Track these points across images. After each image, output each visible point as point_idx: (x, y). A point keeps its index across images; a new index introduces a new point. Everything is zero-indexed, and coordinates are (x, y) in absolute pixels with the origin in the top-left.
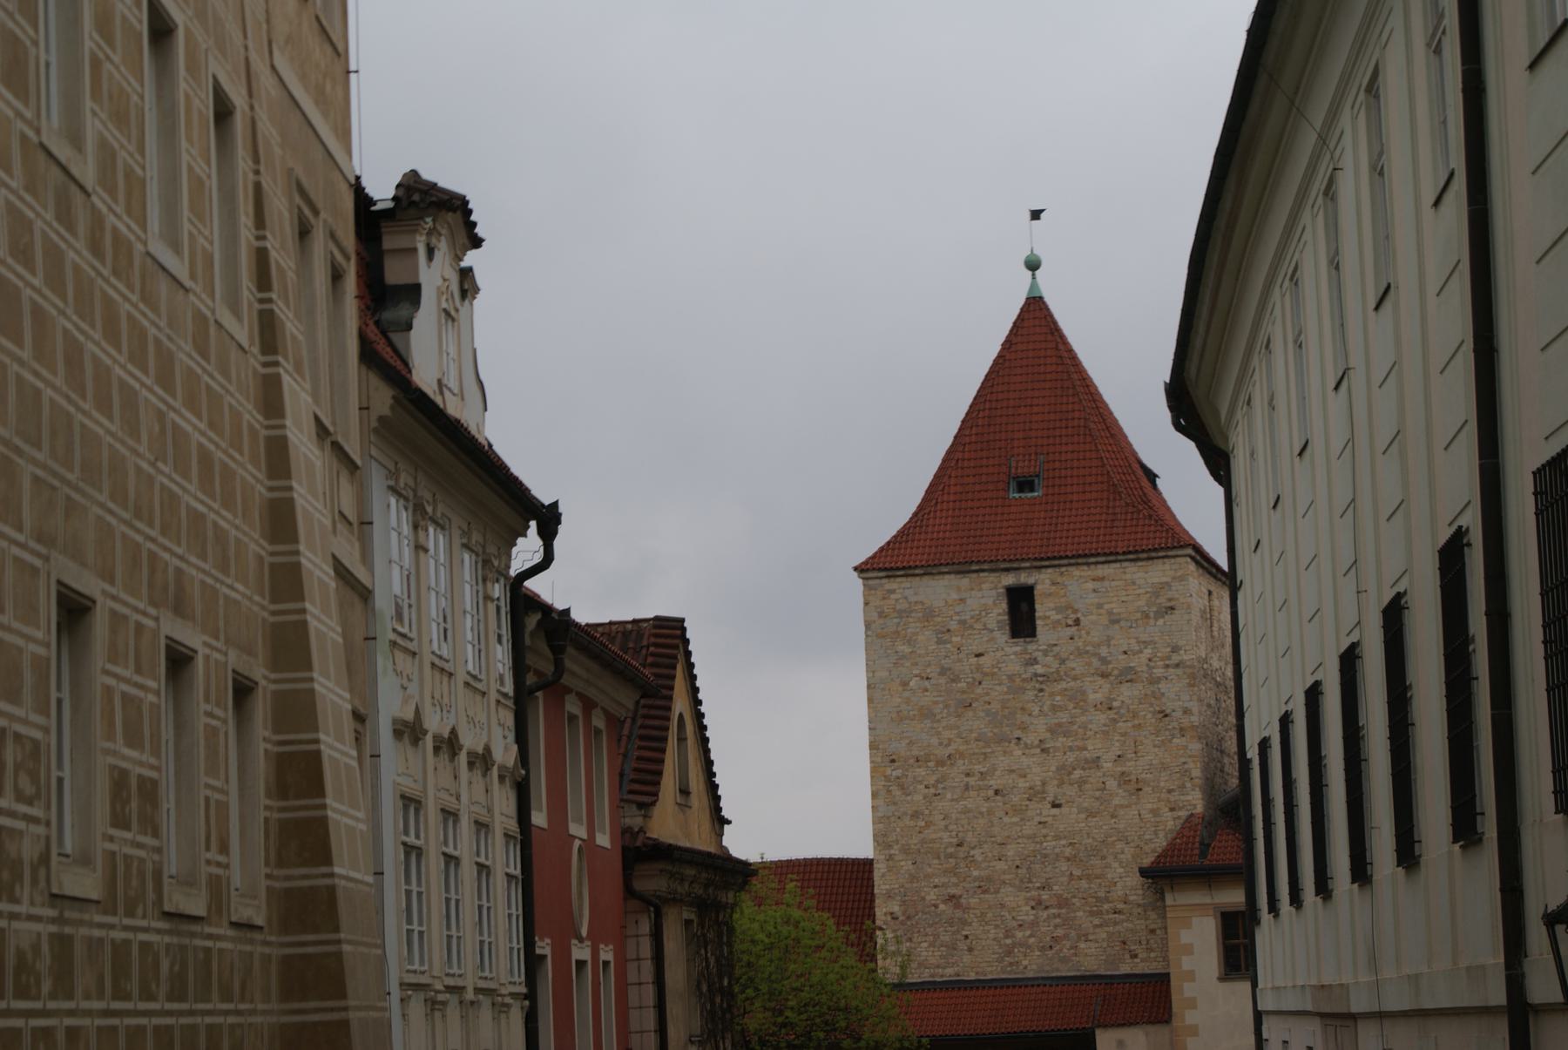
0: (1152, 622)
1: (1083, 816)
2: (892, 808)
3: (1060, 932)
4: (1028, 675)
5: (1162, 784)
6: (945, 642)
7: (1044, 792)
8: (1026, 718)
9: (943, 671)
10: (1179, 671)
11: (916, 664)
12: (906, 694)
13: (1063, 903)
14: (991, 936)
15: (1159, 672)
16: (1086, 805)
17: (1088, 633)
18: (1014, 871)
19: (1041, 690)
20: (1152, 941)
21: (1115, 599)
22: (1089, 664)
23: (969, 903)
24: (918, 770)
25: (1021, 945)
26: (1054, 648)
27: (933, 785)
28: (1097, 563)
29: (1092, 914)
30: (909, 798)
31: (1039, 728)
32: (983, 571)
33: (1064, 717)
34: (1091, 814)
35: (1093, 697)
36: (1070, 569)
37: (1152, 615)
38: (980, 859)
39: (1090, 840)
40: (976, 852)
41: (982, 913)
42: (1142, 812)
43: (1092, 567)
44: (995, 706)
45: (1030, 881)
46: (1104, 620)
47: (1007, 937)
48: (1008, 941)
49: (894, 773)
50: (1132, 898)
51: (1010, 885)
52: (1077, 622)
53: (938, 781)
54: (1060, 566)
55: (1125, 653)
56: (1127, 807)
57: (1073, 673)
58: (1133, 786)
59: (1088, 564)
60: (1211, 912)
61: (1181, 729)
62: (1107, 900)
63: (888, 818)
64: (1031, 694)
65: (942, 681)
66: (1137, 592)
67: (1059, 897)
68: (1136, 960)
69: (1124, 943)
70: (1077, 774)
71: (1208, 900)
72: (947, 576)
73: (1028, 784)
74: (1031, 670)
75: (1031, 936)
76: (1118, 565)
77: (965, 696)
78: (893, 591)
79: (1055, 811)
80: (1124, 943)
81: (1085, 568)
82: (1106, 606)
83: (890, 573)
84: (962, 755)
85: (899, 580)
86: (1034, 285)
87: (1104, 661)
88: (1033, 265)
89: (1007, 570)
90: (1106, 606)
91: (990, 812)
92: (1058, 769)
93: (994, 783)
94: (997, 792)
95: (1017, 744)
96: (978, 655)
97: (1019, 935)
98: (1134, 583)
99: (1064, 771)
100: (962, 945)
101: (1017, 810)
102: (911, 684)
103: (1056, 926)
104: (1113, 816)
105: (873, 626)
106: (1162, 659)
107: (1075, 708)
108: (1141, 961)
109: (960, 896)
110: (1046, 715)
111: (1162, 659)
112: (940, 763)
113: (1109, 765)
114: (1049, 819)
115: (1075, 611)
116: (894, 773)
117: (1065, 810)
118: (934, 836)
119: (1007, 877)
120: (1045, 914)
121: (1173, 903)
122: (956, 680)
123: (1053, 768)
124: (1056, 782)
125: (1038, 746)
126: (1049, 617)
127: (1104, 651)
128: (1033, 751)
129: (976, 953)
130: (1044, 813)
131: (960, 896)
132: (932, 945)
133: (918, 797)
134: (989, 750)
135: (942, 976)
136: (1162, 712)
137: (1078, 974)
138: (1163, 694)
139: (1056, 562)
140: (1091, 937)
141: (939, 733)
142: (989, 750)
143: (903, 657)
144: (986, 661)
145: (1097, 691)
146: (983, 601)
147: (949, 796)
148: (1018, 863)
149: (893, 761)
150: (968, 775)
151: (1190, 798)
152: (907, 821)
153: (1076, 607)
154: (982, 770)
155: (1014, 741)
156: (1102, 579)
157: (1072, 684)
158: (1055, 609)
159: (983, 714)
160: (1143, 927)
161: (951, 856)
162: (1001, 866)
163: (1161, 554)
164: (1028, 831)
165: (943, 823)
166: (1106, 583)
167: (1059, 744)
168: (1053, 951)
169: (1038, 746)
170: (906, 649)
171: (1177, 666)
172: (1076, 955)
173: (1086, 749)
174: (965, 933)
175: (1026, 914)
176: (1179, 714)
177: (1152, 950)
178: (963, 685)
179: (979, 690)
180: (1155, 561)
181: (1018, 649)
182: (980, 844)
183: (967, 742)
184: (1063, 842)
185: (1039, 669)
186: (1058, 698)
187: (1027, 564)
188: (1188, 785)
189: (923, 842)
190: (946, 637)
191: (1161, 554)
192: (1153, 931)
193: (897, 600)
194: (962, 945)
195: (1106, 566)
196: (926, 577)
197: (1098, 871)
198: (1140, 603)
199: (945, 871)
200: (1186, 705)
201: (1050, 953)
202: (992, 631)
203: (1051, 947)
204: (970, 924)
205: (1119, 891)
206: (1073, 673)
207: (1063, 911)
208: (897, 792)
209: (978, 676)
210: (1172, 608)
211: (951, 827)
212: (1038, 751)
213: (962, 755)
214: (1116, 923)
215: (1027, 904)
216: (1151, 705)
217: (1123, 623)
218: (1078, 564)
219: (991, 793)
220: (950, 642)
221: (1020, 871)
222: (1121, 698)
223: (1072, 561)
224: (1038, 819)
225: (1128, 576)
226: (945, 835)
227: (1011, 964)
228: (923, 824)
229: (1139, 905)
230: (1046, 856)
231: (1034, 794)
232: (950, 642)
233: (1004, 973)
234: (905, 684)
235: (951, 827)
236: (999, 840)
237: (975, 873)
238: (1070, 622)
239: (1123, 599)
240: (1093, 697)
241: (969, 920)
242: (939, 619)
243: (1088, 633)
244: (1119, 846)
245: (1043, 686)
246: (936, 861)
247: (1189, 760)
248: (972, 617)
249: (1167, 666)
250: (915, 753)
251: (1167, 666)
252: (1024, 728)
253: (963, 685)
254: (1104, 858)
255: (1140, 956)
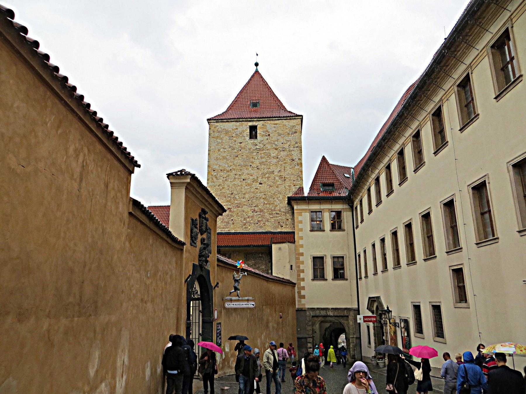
0: (290, 135)
1: (268, 187)
2: (213, 183)
3: (260, 219)
4: (255, 149)
5: (292, 179)
6: (231, 139)
7: (257, 180)
8: (253, 160)
9: (230, 147)
10: (298, 149)
11: (223, 145)
12: (219, 153)
13: (261, 211)
14: (239, 220)
15: (292, 149)
16: (269, 184)
17: (272, 138)
18: (247, 202)
19: (258, 153)
20: (287, 222)
21: (280, 129)
22: (272, 146)
23: (234, 210)
24: (221, 173)
25: (248, 222)
26: (262, 142)
27: (225, 178)
28: (276, 120)
29: (270, 214)
30: (218, 181)
31: (257, 162)
32: (243, 121)
33: (264, 160)
34: (271, 186)
35: (272, 155)
36: (268, 121)
37: (290, 134)
38: (237, 198)
39: (270, 194)
40: (237, 197)
41: (237, 213)
42: (286, 186)
43: (274, 121)
44: (245, 156)
45: (252, 204)
46: (277, 135)
47: (244, 220)
48: (245, 221)
49: (214, 174)
50: (282, 210)
51: (246, 205)
52: (269, 135)
53: (227, 176)
54: (265, 120)
55: (282, 143)
56: (281, 184)
57: (267, 148)
58: (283, 179)
59: (273, 120)
60: (308, 211)
61: (298, 164)
62: (274, 210)
63: (212, 186)
64: (255, 154)
65: (230, 149)
66: (287, 128)
67: (260, 209)
68: (282, 228)
69: (279, 223)
70: (267, 175)
71: (307, 208)
72: (233, 122)
73: (253, 178)
74: (255, 147)
75: (251, 220)
76: (281, 121)
77: (236, 154)
78: (217, 126)
79: (261, 185)
80: (279, 223)
81: (272, 121)
82: (277, 131)
83: (217, 121)
84: (234, 170)
85: (219, 123)
86: (257, 69)
87: (276, 145)
88: (257, 65)
89: (250, 121)
90: (277, 131)
91: (241, 185)
92: (262, 174)
93: (243, 177)
94: (243, 180)
95: (250, 167)
96: (240, 143)
97: (248, 220)
98: (285, 125)
99: (263, 175)
100: (231, 222)
101: (249, 185)
102: (221, 150)
103: (259, 217)
104: (277, 187)
105: (211, 135)
106: (293, 145)
107: (267, 158)
108: (284, 228)
109: (231, 208)
110: (259, 159)
111: (293, 145)
112: (228, 171)
113: (277, 173)
114: (259, 188)
115: (269, 132)
116: (214, 174)
117: (263, 185)
118: (225, 191)
119: (245, 203)
120: (256, 214)
121: (297, 208)
122: (234, 149)
123: (260, 174)
124: (261, 177)
125: (256, 168)
126: (261, 134)
127: (276, 143)
128: (255, 169)
129: (235, 224)
130: (257, 186)
131: (231, 208)
132: (222, 222)
133: (221, 181)
134: (242, 168)
135: (224, 231)
136: (292, 159)
137: (265, 231)
138: (293, 154)
139: (264, 119)
140: (269, 221)
141: (228, 163)
142: (242, 168)
143: (219, 143)
144: (243, 145)
145: (274, 153)
146: (243, 129)
147: (230, 180)
148: (249, 199)
149: (214, 171)
150: (236, 175)
151: (300, 183)
152: (217, 187)
153: (269, 131)
154: (240, 174)
155: (249, 166)
156: (277, 124)
157: (267, 151)
158: (263, 132)
159: (241, 159)
160: (285, 218)
161: (229, 197)
162: (244, 200)
163: (293, 118)
164: (252, 190)
165: (228, 188)
166: (278, 125)
167: (262, 167)
168: (258, 225)
169: (256, 168)
170: (221, 141)
171: (297, 147)
172: (265, 226)
173: (270, 168)
174: (232, 219)
175: (250, 214)
176: (297, 160)
177: (287, 225)
178: (236, 151)
179: (240, 152)
180: (292, 120)
181: (252, 142)
182: (238, 194)
183: (236, 166)
184: (262, 194)
185: (258, 147)
186: (263, 155)
187: (256, 120)
188: (299, 179)
189: (221, 193)
190: (232, 138)
191: (293, 118)
192: (288, 220)
193: (218, 128)
194: (231, 222)
195: (278, 121)
196: (227, 123)
197: (272, 202)
198: (286, 131)
199: (227, 201)
200: (299, 157)
201: (257, 225)
202: (245, 137)
203: (257, 223)
204: (234, 216)
205: (278, 208)
206: (267, 148)
207: (261, 213)
208: (214, 179)
209: (240, 148)
210: (296, 132)
211: (230, 189)
212: (256, 169)
213: (234, 170)
214: (277, 217)
215: (251, 211)
216: (289, 157)
217: (282, 136)
218: (270, 120)
219: (242, 180)
220: (233, 139)
221: (249, 202)
222: (281, 155)
223: (269, 119)
224: (255, 187)
225: (284, 124)
226: (228, 191)
227: (245, 228)
228: (222, 188)
229: (284, 212)
230: (257, 197)
231: (254, 181)
232: (233, 139)
233: (243, 230)
234: (219, 150)
235: (230, 189)
236: (244, 193)
237: (236, 202)
238: (267, 135)
239: (282, 129)
240: (272, 155)
241: (233, 215)
242: (230, 133)
243: (272, 138)
244: (278, 195)
245: (259, 152)
246: (225, 198)
247: (300, 172)
248: (239, 133)
249: (294, 147)
250: (221, 168)
251: (294, 147)
252: (253, 163)
253: (236, 151)
254: (274, 198)
255: (284, 226)
